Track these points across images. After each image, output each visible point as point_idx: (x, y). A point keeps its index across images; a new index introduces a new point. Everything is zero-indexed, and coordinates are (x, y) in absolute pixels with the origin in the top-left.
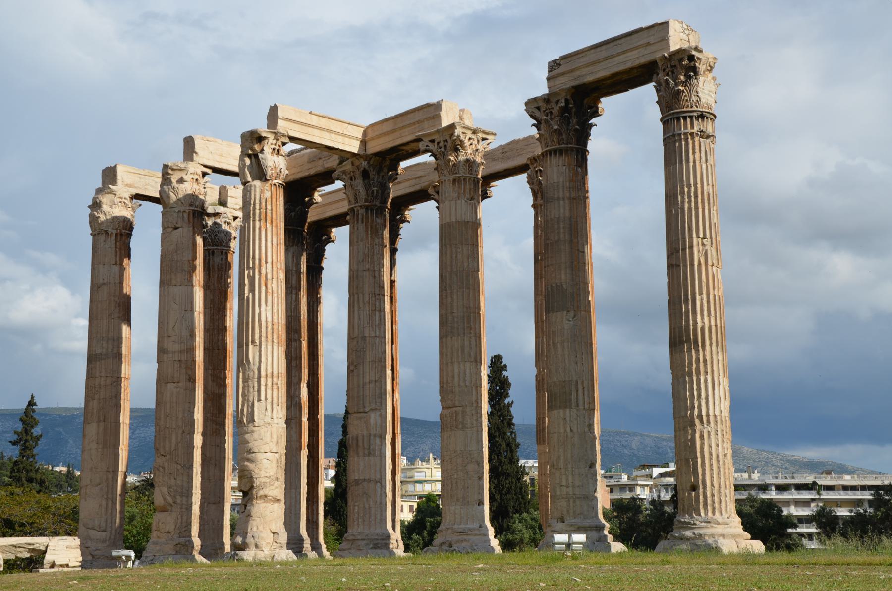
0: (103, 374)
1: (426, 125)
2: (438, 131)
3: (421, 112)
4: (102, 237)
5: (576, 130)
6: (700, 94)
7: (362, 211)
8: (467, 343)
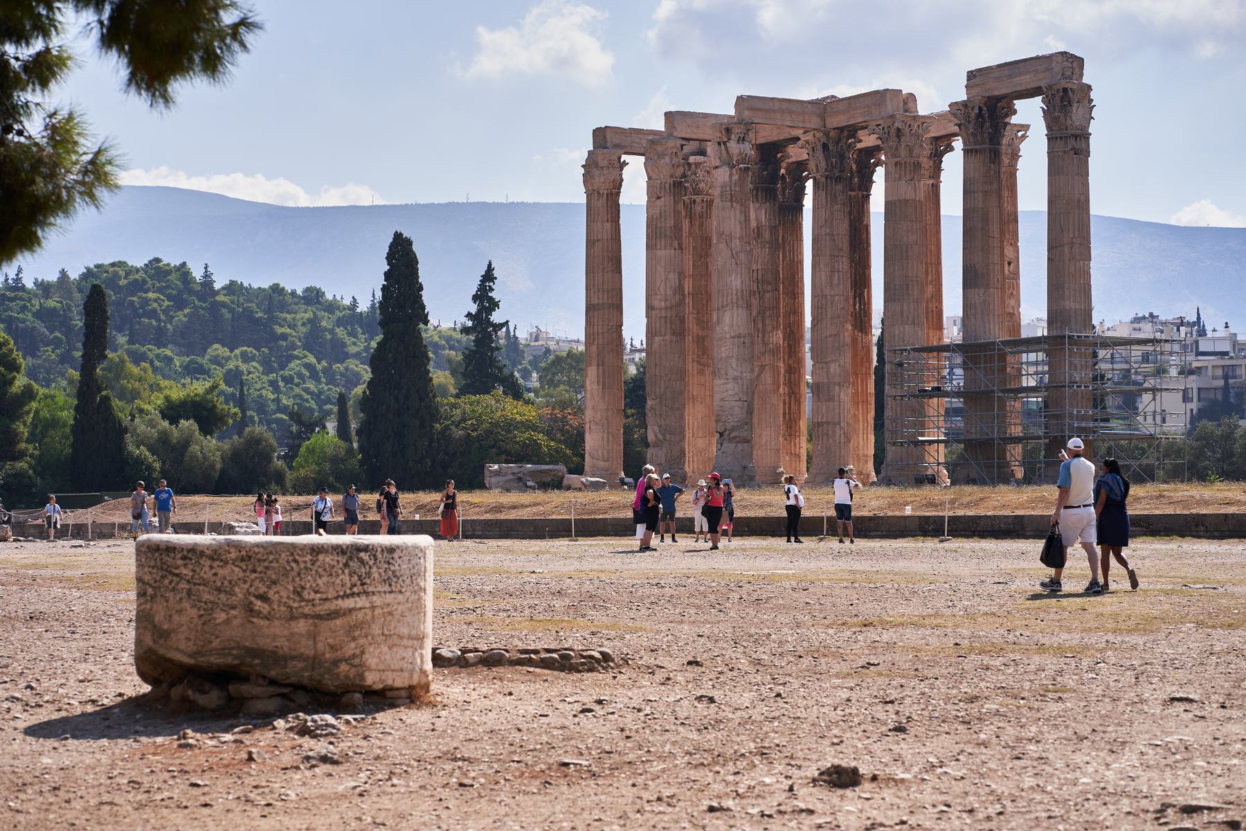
0: (601, 323)
5: (989, 133)
6: (1074, 118)
7: (824, 179)
8: (905, 308)
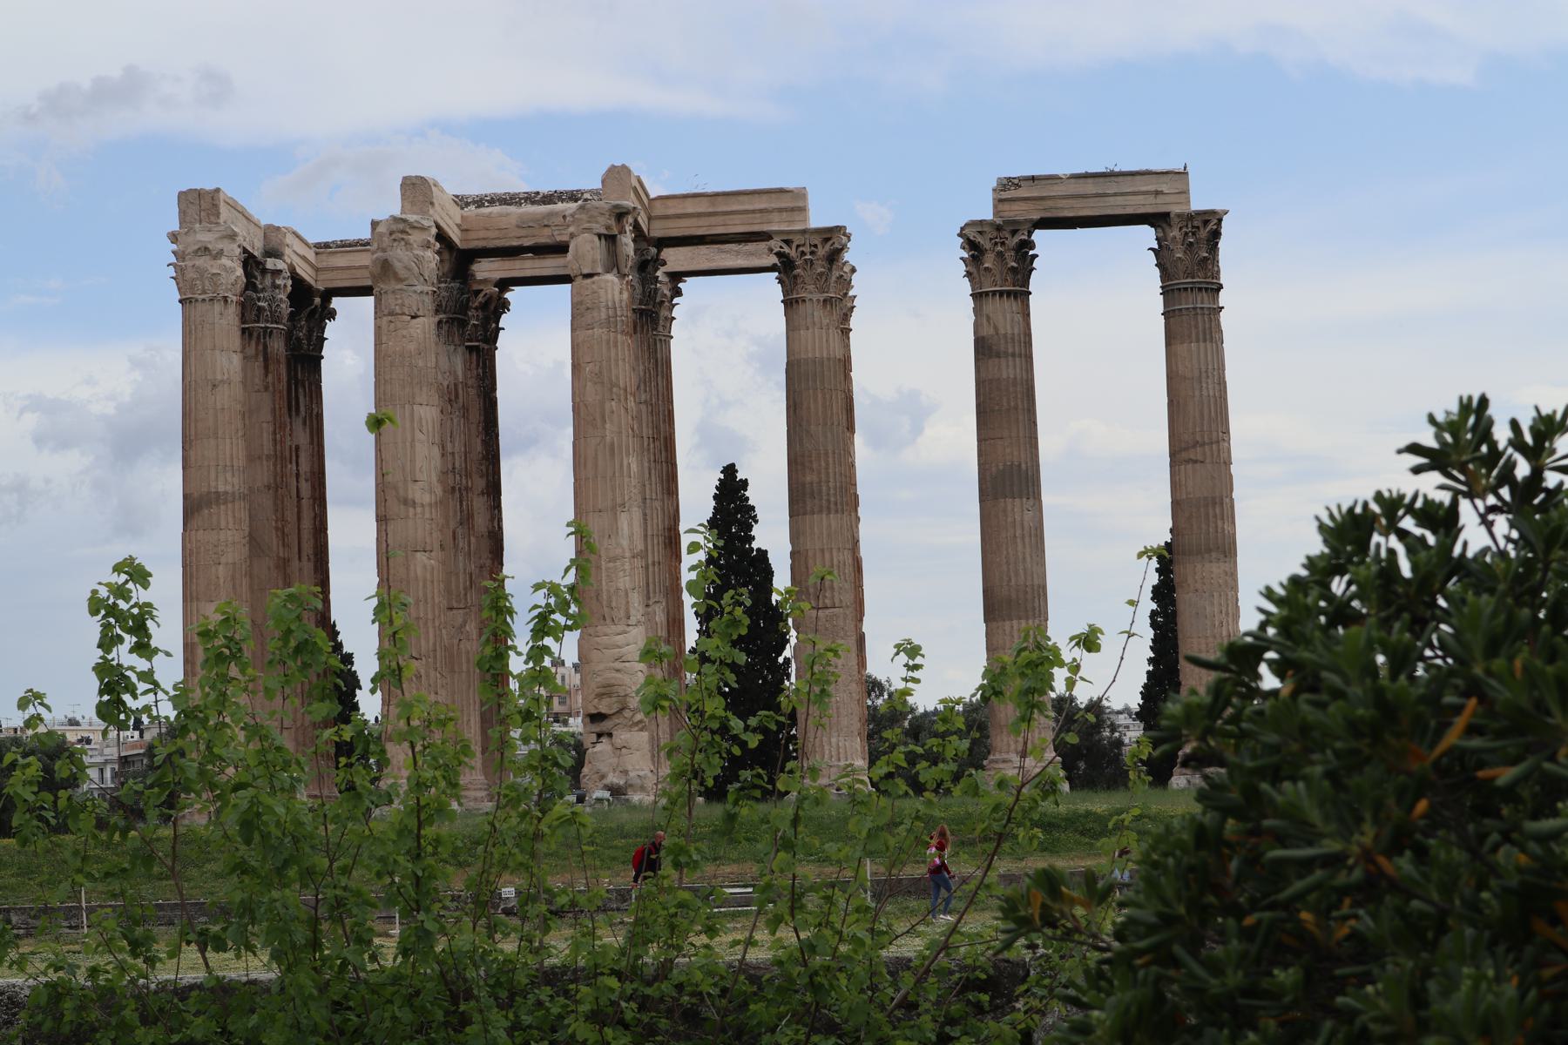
1: (775, 216)
2: (804, 232)
3: (765, 197)
4: (218, 307)
